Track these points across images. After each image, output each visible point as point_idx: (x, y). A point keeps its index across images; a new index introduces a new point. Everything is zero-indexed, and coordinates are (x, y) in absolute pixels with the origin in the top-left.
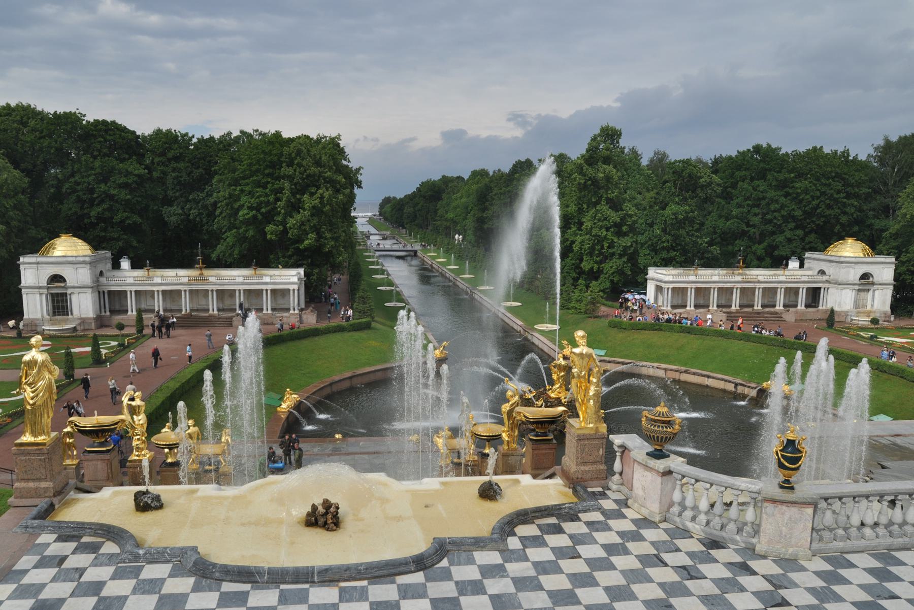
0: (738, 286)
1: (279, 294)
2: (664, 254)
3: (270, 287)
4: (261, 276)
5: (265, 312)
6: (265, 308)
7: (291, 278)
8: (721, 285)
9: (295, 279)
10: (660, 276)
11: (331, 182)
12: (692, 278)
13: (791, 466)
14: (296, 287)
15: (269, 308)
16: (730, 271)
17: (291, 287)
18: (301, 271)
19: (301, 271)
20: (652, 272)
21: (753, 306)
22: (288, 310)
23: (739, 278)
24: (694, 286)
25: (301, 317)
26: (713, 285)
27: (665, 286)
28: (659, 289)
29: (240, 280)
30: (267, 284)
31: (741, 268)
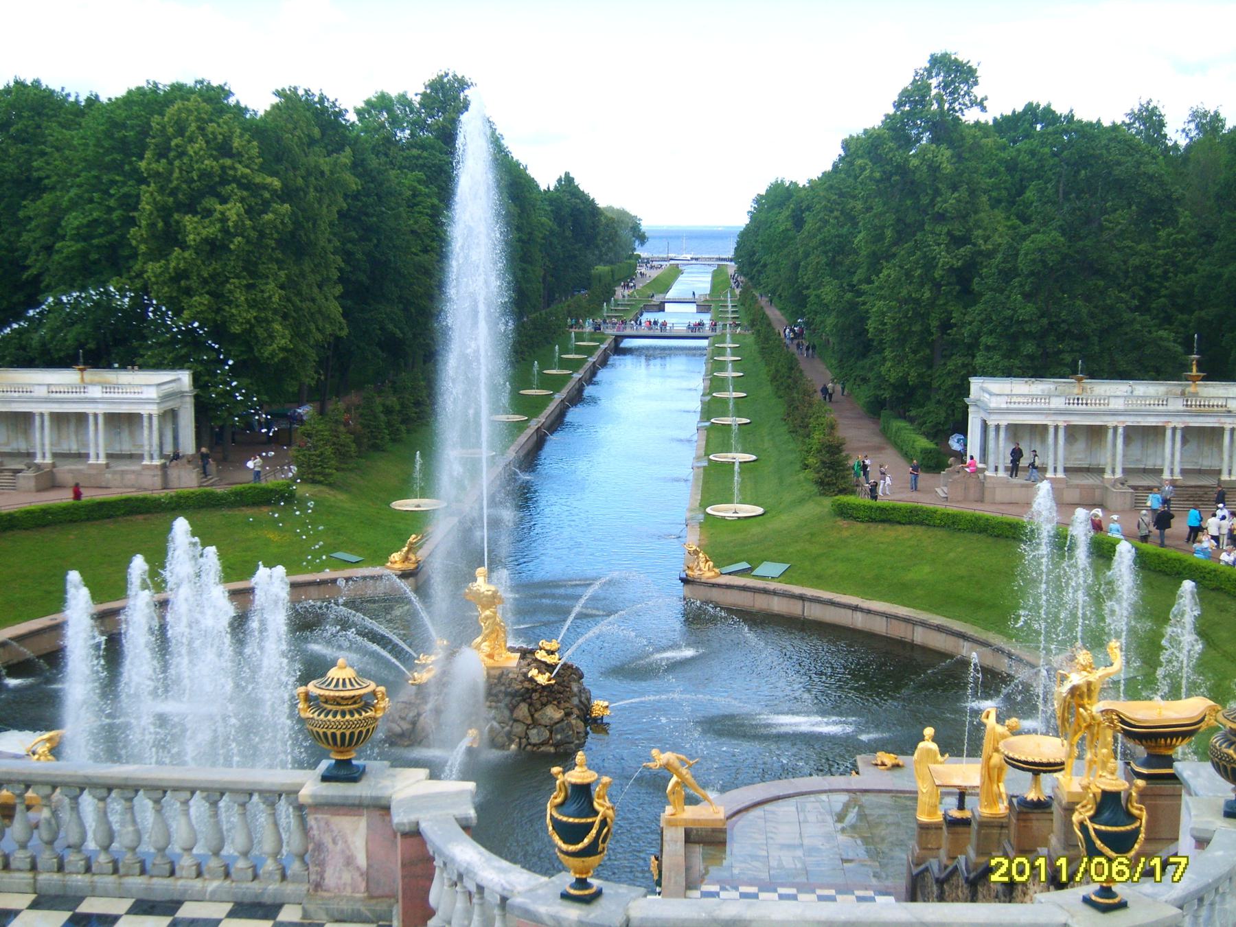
0: (1179, 423)
1: (122, 422)
2: (1029, 348)
3: (101, 409)
4: (84, 385)
5: (92, 461)
6: (92, 453)
7: (146, 389)
8: (1131, 421)
9: (153, 393)
10: (997, 398)
11: (246, 185)
12: (1058, 403)
13: (572, 848)
14: (154, 410)
15: (102, 455)
16: (1173, 386)
17: (145, 410)
18: (184, 378)
19: (184, 378)
20: (976, 384)
21: (1219, 472)
22: (141, 457)
23: (1178, 405)
24: (1061, 421)
25: (165, 476)
26: (1110, 422)
27: (992, 422)
28: (985, 426)
29: (42, 392)
30: (93, 401)
31: (1194, 379)
